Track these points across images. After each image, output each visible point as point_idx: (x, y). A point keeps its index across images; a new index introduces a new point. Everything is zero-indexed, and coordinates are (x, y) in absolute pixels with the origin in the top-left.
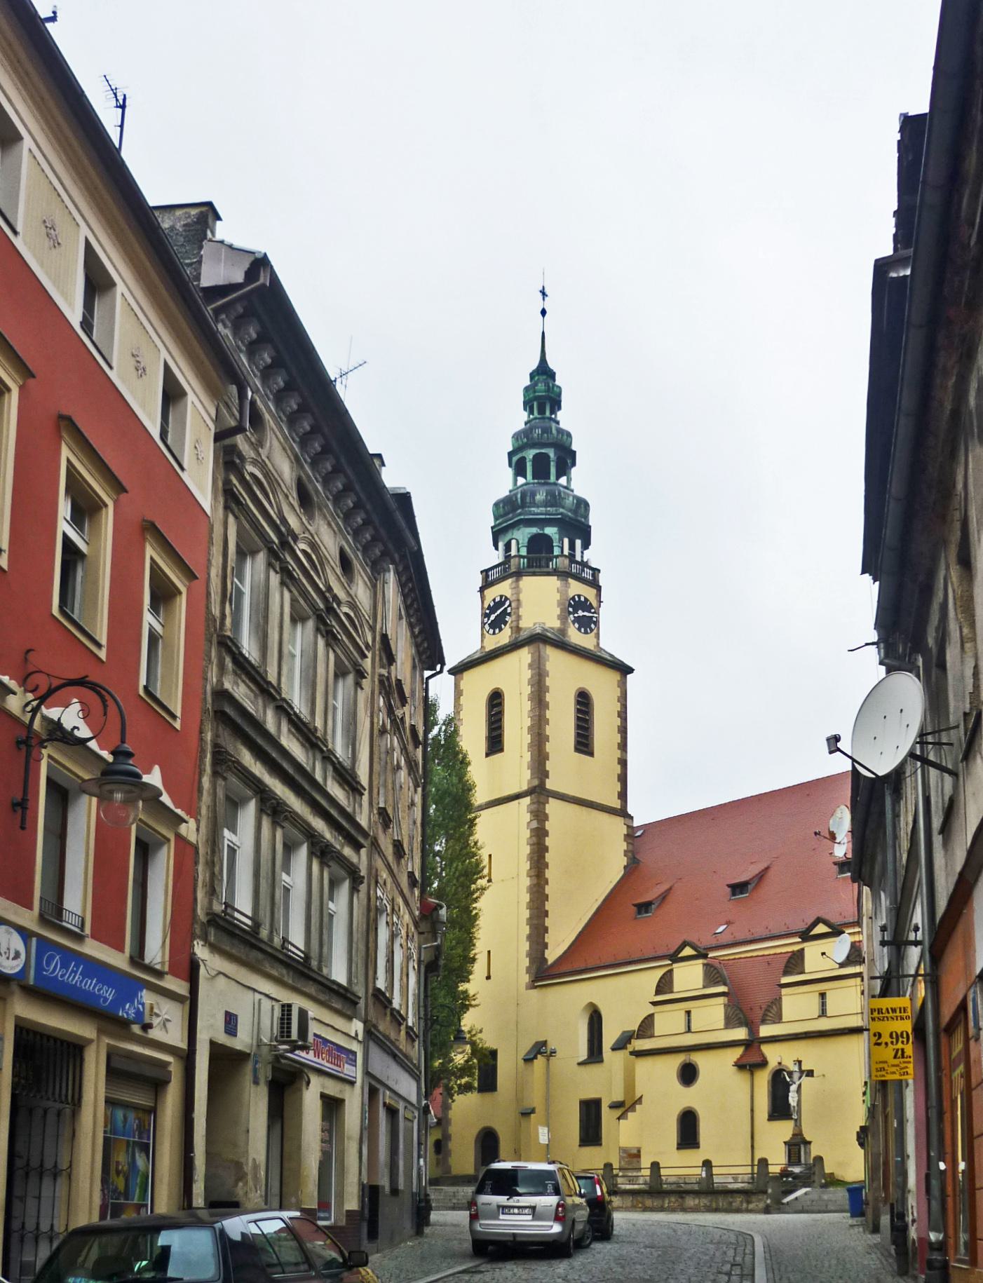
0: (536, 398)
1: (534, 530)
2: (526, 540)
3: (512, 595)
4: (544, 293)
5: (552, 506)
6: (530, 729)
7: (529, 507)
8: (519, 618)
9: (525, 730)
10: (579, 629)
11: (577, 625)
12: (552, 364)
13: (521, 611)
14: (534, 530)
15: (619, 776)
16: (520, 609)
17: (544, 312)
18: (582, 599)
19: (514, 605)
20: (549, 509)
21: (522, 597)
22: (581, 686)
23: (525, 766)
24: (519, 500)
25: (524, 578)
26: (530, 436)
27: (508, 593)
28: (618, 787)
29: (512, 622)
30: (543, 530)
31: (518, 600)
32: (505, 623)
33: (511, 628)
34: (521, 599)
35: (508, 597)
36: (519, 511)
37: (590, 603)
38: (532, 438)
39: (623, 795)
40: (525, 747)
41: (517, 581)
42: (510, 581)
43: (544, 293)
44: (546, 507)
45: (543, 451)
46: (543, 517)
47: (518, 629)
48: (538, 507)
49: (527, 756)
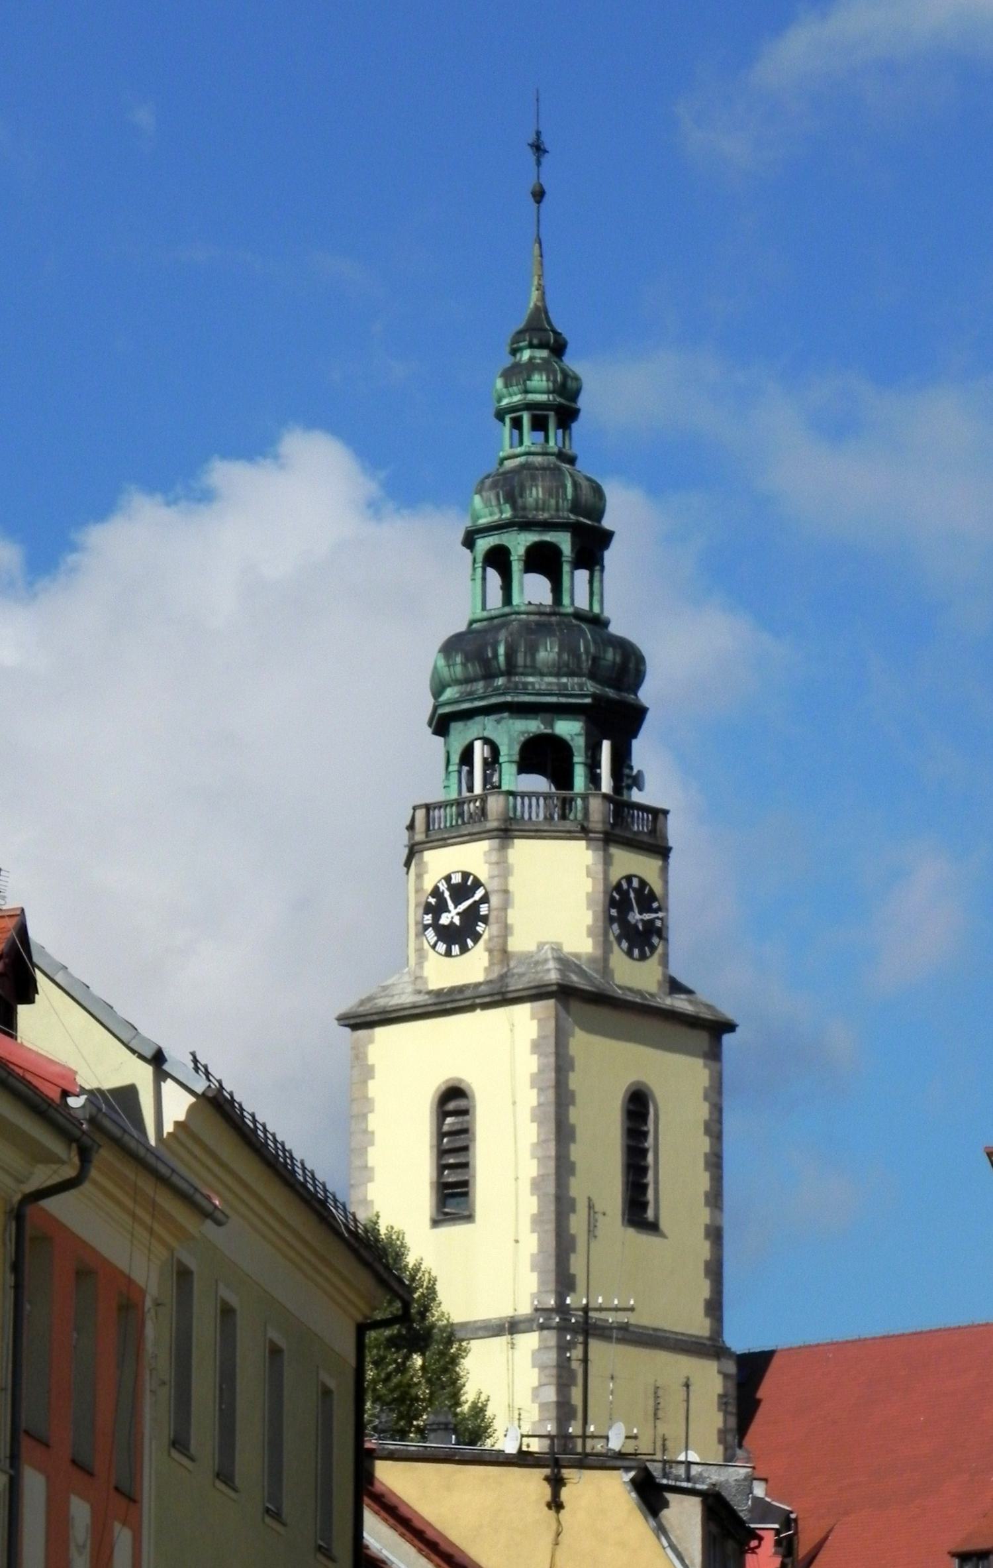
0: (529, 406)
1: (534, 726)
2: (517, 748)
3: (492, 877)
4: (538, 148)
5: (571, 674)
6: (536, 1185)
7: (523, 674)
8: (506, 930)
9: (525, 1186)
10: (629, 953)
11: (625, 945)
12: (561, 323)
13: (513, 916)
14: (534, 726)
15: (707, 1265)
16: (510, 912)
17: (539, 195)
18: (635, 883)
19: (495, 900)
20: (564, 680)
21: (513, 884)
22: (643, 1079)
23: (525, 1262)
24: (502, 659)
25: (516, 841)
26: (520, 501)
27: (482, 872)
28: (704, 1289)
29: (491, 939)
30: (552, 727)
31: (506, 892)
32: (477, 937)
33: (490, 951)
34: (511, 888)
35: (483, 878)
36: (500, 681)
37: (651, 891)
38: (524, 508)
39: (714, 1308)
40: (526, 1223)
41: (503, 848)
42: (485, 845)
43: (538, 148)
44: (558, 675)
45: (549, 537)
46: (553, 699)
47: (501, 953)
48: (542, 675)
49: (530, 1243)
